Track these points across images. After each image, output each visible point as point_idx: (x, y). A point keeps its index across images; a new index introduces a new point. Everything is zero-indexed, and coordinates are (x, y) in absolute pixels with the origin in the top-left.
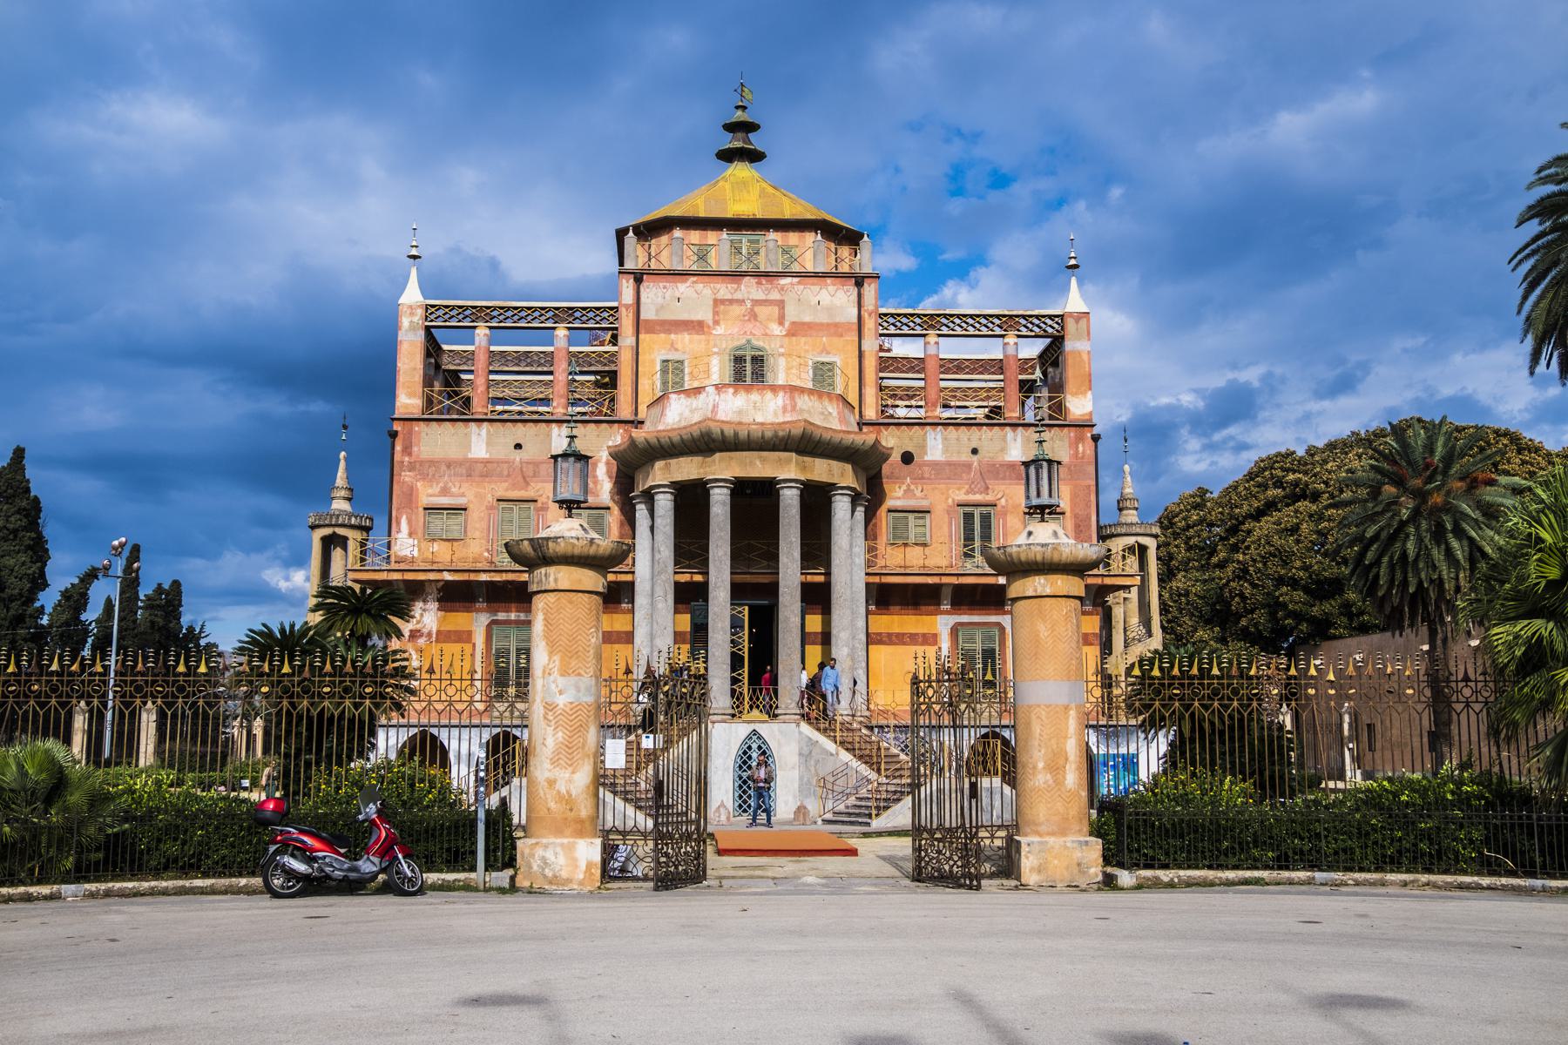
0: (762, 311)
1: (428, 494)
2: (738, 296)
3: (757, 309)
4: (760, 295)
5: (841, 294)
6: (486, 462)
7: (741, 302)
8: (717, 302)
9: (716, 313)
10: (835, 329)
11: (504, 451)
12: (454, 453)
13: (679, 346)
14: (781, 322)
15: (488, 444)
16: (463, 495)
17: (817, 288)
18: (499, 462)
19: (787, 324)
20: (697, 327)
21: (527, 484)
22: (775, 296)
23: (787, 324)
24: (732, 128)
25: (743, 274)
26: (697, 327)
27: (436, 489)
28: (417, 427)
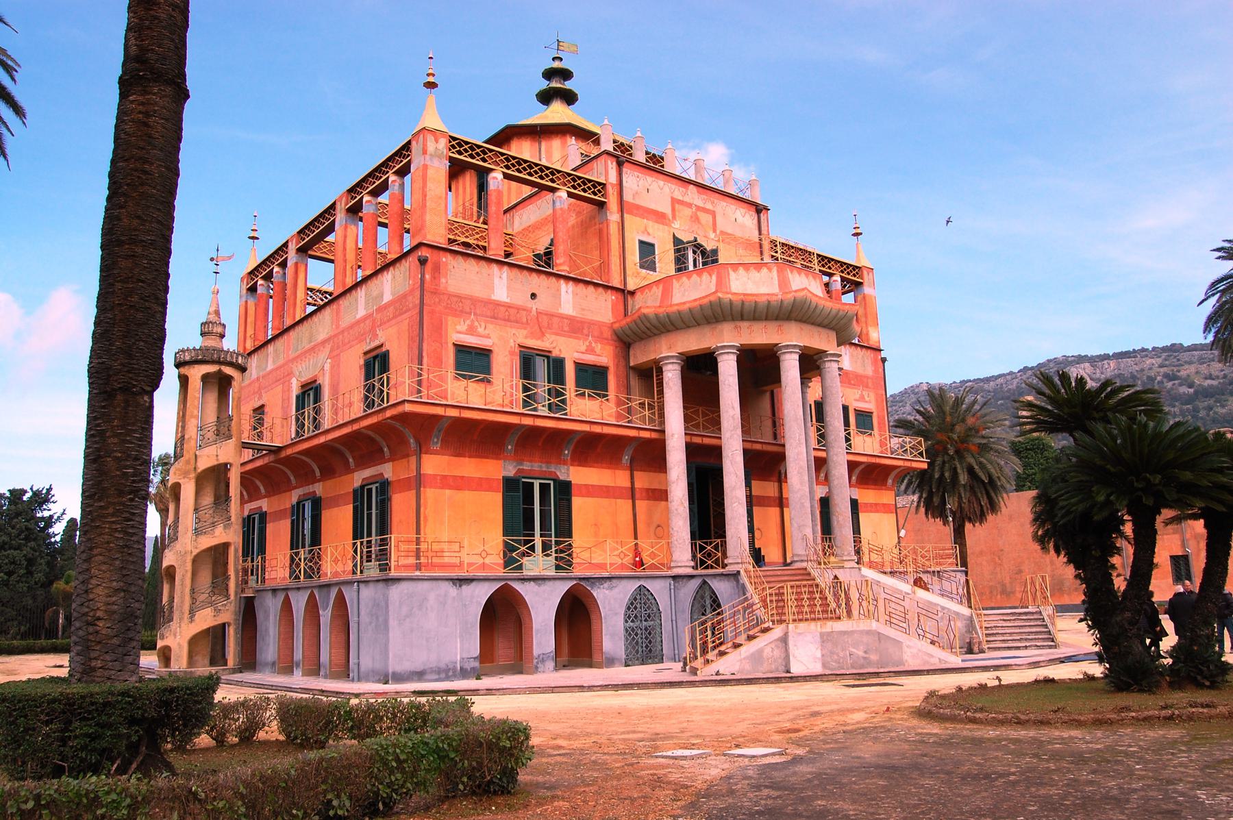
0: (701, 215)
1: (459, 333)
2: (687, 199)
4: (701, 204)
5: (747, 216)
6: (508, 306)
7: (689, 205)
8: (674, 201)
9: (673, 210)
10: (747, 244)
11: (522, 299)
12: (478, 291)
13: (650, 230)
14: (715, 231)
15: (509, 288)
16: (488, 337)
18: (519, 309)
20: (659, 217)
21: (543, 334)
22: (709, 206)
24: (549, 74)
25: (690, 182)
26: (659, 217)
28: (446, 259)
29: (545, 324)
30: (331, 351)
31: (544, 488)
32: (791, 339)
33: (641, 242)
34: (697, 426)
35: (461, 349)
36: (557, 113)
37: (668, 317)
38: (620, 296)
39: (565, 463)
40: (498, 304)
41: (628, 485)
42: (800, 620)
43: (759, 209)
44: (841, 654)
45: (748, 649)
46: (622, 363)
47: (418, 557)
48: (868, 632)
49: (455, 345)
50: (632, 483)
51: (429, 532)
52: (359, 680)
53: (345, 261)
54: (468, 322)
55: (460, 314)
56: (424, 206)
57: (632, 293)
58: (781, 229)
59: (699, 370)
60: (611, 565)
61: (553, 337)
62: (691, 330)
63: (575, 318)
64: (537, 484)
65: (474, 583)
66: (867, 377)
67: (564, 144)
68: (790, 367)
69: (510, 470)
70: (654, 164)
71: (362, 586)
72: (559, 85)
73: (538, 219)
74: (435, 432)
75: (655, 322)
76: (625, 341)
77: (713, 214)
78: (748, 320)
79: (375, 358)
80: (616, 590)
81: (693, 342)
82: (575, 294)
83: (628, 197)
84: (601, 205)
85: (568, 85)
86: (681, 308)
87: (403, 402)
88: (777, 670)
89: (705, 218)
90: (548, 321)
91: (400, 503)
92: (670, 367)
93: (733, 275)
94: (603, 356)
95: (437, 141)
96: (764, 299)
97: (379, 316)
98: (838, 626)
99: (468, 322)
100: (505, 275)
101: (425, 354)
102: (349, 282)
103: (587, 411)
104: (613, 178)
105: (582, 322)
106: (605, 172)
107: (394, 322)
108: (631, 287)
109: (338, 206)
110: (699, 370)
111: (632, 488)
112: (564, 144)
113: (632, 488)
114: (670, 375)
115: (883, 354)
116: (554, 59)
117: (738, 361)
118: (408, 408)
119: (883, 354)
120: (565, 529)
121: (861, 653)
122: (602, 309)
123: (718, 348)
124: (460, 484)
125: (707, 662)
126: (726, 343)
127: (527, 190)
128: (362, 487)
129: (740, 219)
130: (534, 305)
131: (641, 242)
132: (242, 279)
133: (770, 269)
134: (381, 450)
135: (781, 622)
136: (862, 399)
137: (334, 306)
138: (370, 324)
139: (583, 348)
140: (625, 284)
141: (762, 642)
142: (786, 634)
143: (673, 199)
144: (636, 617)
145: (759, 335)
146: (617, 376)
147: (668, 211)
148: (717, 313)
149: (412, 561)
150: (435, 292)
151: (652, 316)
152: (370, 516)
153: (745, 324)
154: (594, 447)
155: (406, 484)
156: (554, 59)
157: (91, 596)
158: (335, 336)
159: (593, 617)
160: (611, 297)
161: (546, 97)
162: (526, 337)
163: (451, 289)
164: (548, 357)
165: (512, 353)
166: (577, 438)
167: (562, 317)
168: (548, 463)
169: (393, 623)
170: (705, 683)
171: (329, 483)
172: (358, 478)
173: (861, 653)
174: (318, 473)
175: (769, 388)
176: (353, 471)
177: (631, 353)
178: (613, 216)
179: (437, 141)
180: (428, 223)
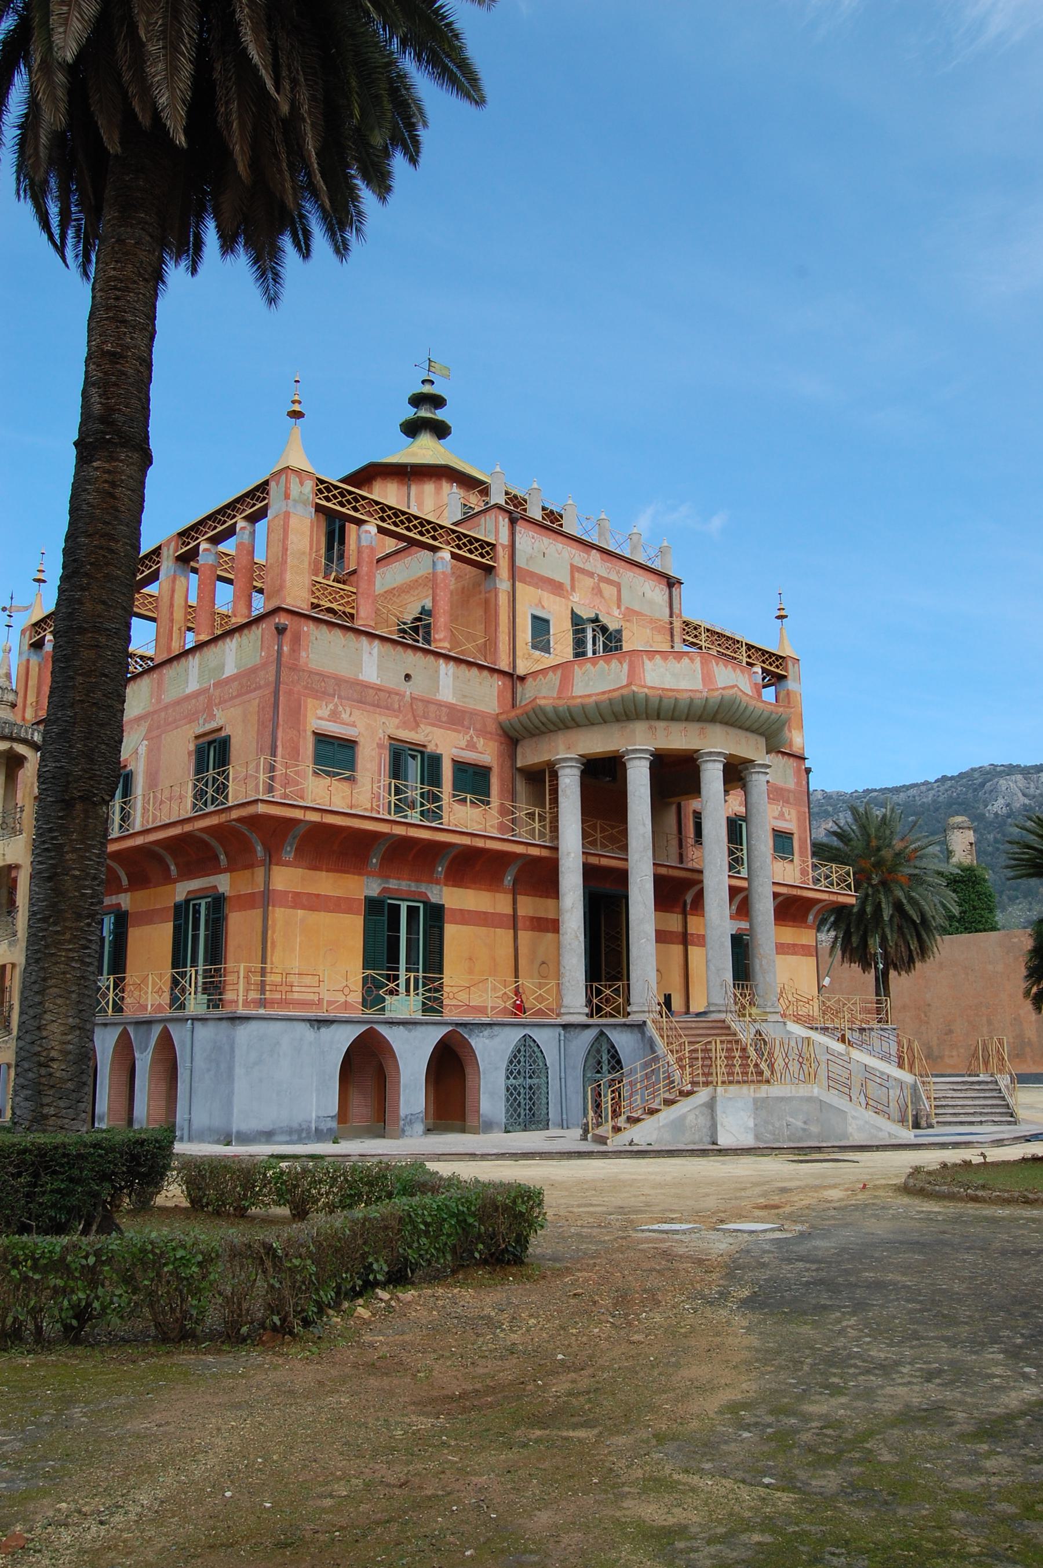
1: (320, 718)
2: (588, 567)
3: (603, 585)
6: (378, 689)
7: (591, 574)
8: (574, 569)
9: (573, 579)
11: (395, 681)
12: (344, 670)
13: (546, 604)
14: (619, 607)
17: (642, 579)
18: (390, 693)
19: (623, 609)
21: (418, 725)
22: (614, 577)
23: (623, 609)
24: (418, 400)
25: (592, 546)
26: (556, 588)
27: (324, 712)
29: (420, 712)
30: (150, 730)
31: (412, 912)
32: (716, 744)
33: (535, 618)
34: (593, 843)
35: (322, 739)
36: (426, 450)
37: (569, 710)
38: (508, 681)
39: (438, 883)
40: (366, 686)
41: (509, 911)
42: (731, 1082)
43: (672, 583)
44: (777, 1125)
45: (667, 1115)
46: (508, 764)
47: (263, 991)
48: (810, 1099)
49: (314, 733)
50: (515, 909)
51: (277, 959)
52: (190, 1140)
53: (172, 620)
54: (331, 706)
55: (321, 695)
56: (284, 562)
57: (522, 679)
58: (698, 606)
59: (603, 776)
60: (493, 1008)
61: (429, 729)
62: (595, 728)
63: (453, 705)
64: (404, 907)
65: (334, 1027)
66: (789, 791)
67: (438, 490)
68: (712, 775)
69: (373, 888)
70: (551, 523)
71: (197, 1024)
72: (429, 415)
73: (401, 581)
74: (289, 839)
75: (552, 715)
76: (512, 738)
77: (618, 586)
78: (665, 719)
79: (210, 743)
80: (497, 1040)
81: (597, 743)
82: (456, 677)
83: (520, 562)
84: (489, 570)
85: (440, 415)
86: (587, 700)
87: (256, 801)
88: (701, 1141)
89: (609, 591)
90: (422, 709)
91: (239, 925)
92: (568, 771)
93: (648, 664)
94: (486, 753)
95: (302, 484)
96: (686, 695)
97: (218, 692)
98: (764, 1091)
99: (331, 706)
100: (375, 651)
101: (279, 743)
102: (176, 649)
103: (466, 820)
104: (504, 538)
105: (463, 712)
106: (494, 529)
107: (237, 701)
108: (521, 671)
109: (164, 551)
110: (603, 776)
111: (515, 916)
112: (438, 490)
113: (515, 916)
114: (567, 781)
115: (808, 764)
116: (423, 382)
117: (651, 768)
118: (261, 808)
119: (808, 764)
120: (435, 963)
121: (800, 1124)
122: (485, 696)
123: (628, 752)
124: (315, 903)
125: (617, 1130)
126: (638, 746)
127: (391, 545)
128: (187, 901)
129: (649, 594)
130: (408, 689)
131: (535, 618)
132: (23, 632)
133: (692, 660)
134: (216, 858)
135: (707, 1084)
136: (781, 816)
137: (155, 675)
138: (207, 700)
139: (463, 744)
140: (514, 667)
141: (684, 1106)
142: (713, 1099)
143: (572, 565)
144: (519, 1073)
145: (678, 739)
146: (502, 780)
147: (566, 580)
148: (627, 710)
149: (253, 995)
150: (294, 668)
151: (549, 709)
152: (196, 938)
153: (661, 724)
154: (472, 864)
155: (248, 902)
156: (423, 382)
157: (45, 1034)
158: (155, 712)
159: (469, 1071)
160: (497, 683)
161: (412, 429)
162: (398, 728)
163: (313, 665)
164: (422, 753)
165: (380, 746)
166: (454, 852)
167: (440, 704)
168: (417, 881)
169: (239, 1071)
170: (618, 1154)
171: (140, 894)
172: (181, 891)
173: (800, 1124)
174: (125, 882)
175: (676, 799)
176: (175, 881)
177: (519, 750)
178: (503, 584)
179: (302, 484)
180: (288, 584)
